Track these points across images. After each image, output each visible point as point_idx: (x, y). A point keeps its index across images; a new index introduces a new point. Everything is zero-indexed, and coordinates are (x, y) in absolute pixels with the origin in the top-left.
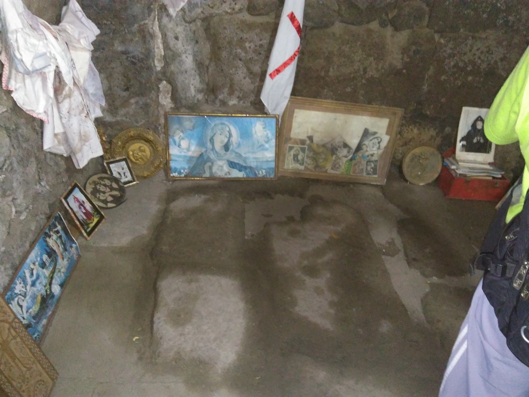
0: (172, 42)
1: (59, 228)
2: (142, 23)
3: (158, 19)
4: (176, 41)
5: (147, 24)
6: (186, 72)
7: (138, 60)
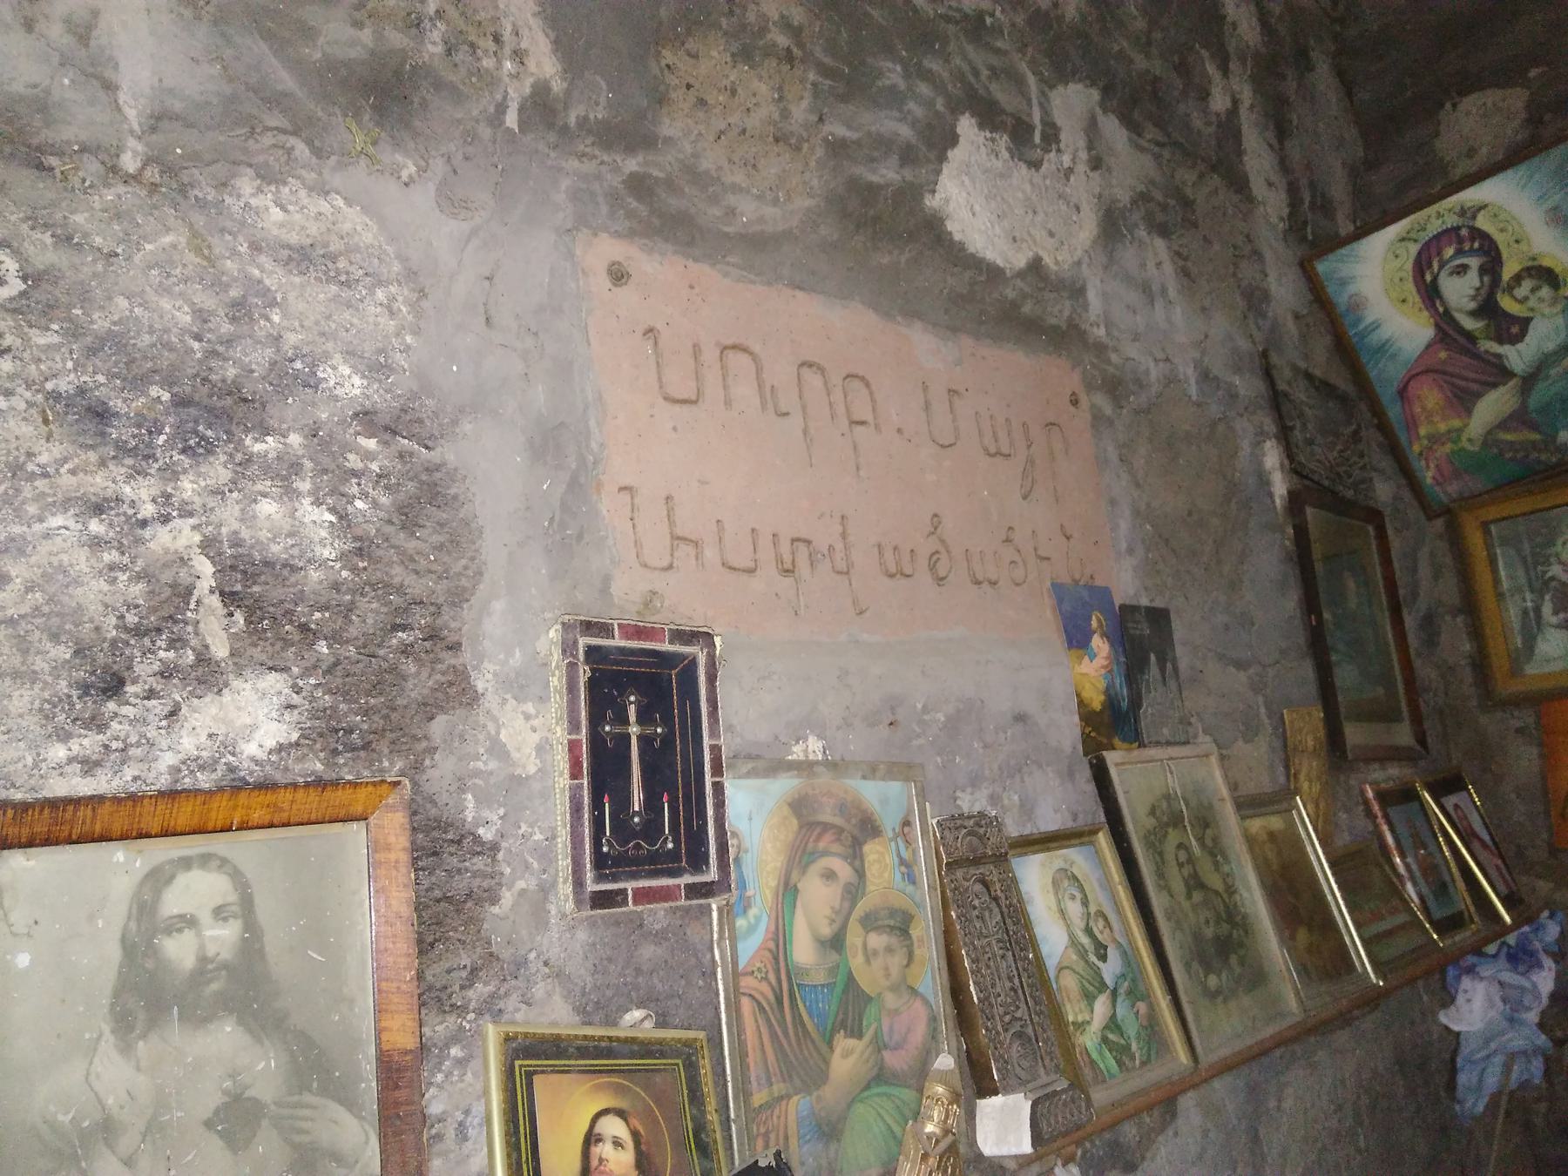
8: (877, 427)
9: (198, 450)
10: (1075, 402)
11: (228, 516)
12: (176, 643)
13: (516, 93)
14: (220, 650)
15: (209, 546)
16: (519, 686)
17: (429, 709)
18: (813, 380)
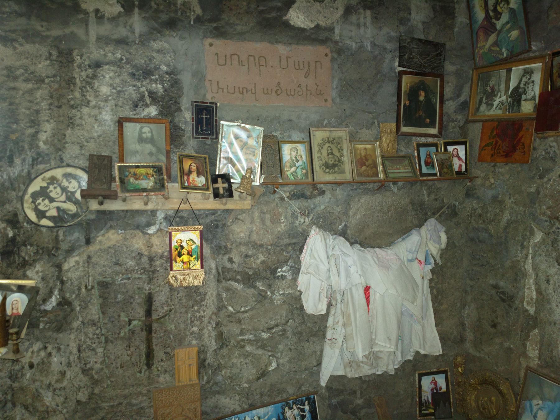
0: (543, 286)
1: (307, 408)
2: (515, 259)
3: (532, 258)
5: (519, 261)
6: (555, 324)
7: (508, 297)
8: (266, 66)
9: (145, 78)
11: (149, 87)
12: (143, 102)
13: (192, 18)
14: (149, 103)
15: (147, 90)
16: (187, 109)
17: (175, 112)
18: (251, 59)
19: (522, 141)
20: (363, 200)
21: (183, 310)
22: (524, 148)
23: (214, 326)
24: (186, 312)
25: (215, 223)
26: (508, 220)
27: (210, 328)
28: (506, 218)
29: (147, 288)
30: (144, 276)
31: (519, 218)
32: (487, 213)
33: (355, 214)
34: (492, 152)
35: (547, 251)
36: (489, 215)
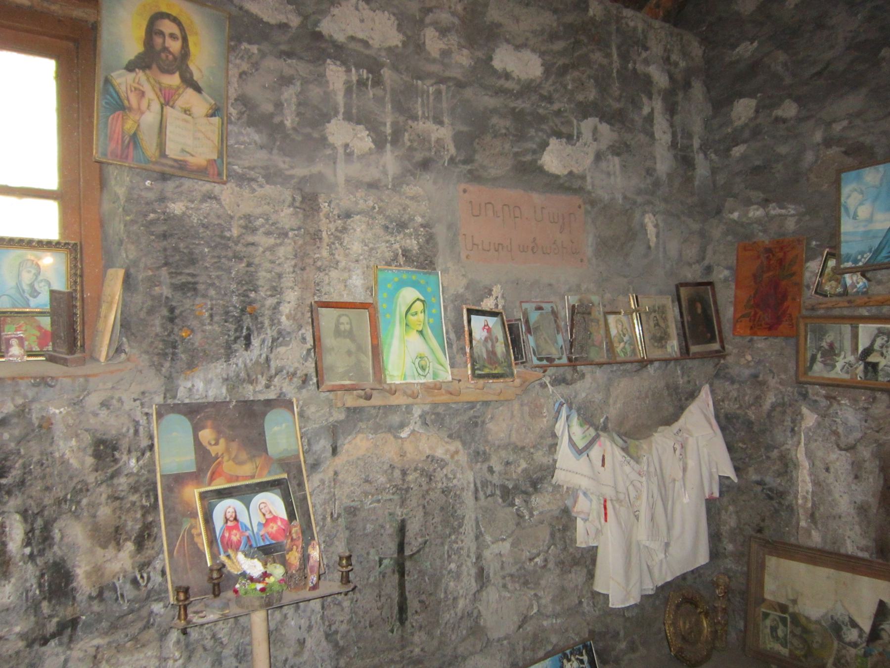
3: (805, 444)
4: (827, 474)
5: (789, 450)
6: (840, 517)
8: (521, 218)
9: (399, 232)
10: (580, 207)
13: (447, 158)
14: (402, 263)
18: (506, 208)
19: (788, 312)
20: (622, 385)
21: (439, 541)
22: (792, 320)
23: (474, 560)
24: (443, 544)
25: (474, 420)
26: (772, 403)
27: (469, 564)
28: (770, 401)
29: (400, 514)
30: (396, 497)
31: (786, 399)
32: (744, 395)
33: (615, 403)
34: (751, 324)
35: (824, 435)
36: (747, 398)
